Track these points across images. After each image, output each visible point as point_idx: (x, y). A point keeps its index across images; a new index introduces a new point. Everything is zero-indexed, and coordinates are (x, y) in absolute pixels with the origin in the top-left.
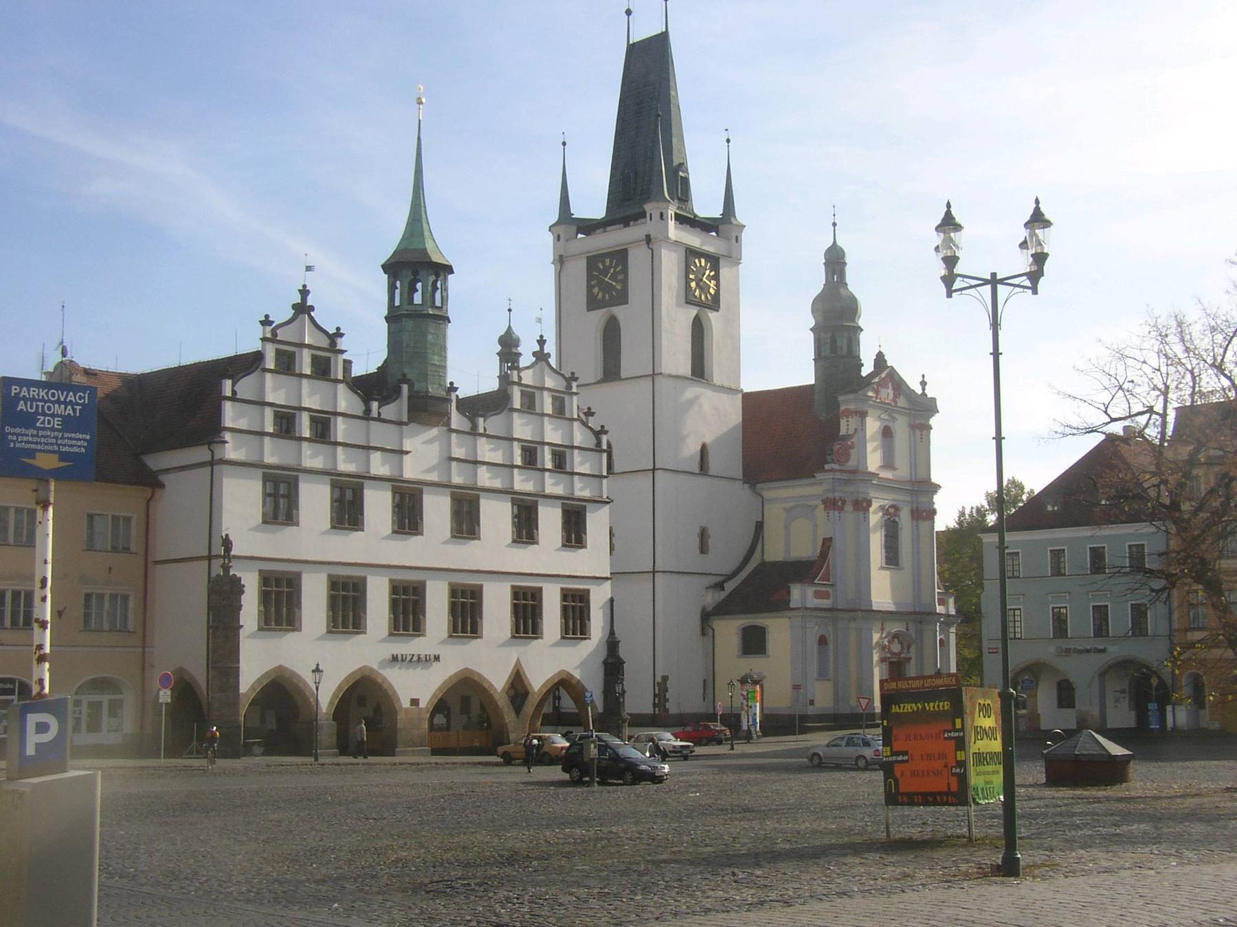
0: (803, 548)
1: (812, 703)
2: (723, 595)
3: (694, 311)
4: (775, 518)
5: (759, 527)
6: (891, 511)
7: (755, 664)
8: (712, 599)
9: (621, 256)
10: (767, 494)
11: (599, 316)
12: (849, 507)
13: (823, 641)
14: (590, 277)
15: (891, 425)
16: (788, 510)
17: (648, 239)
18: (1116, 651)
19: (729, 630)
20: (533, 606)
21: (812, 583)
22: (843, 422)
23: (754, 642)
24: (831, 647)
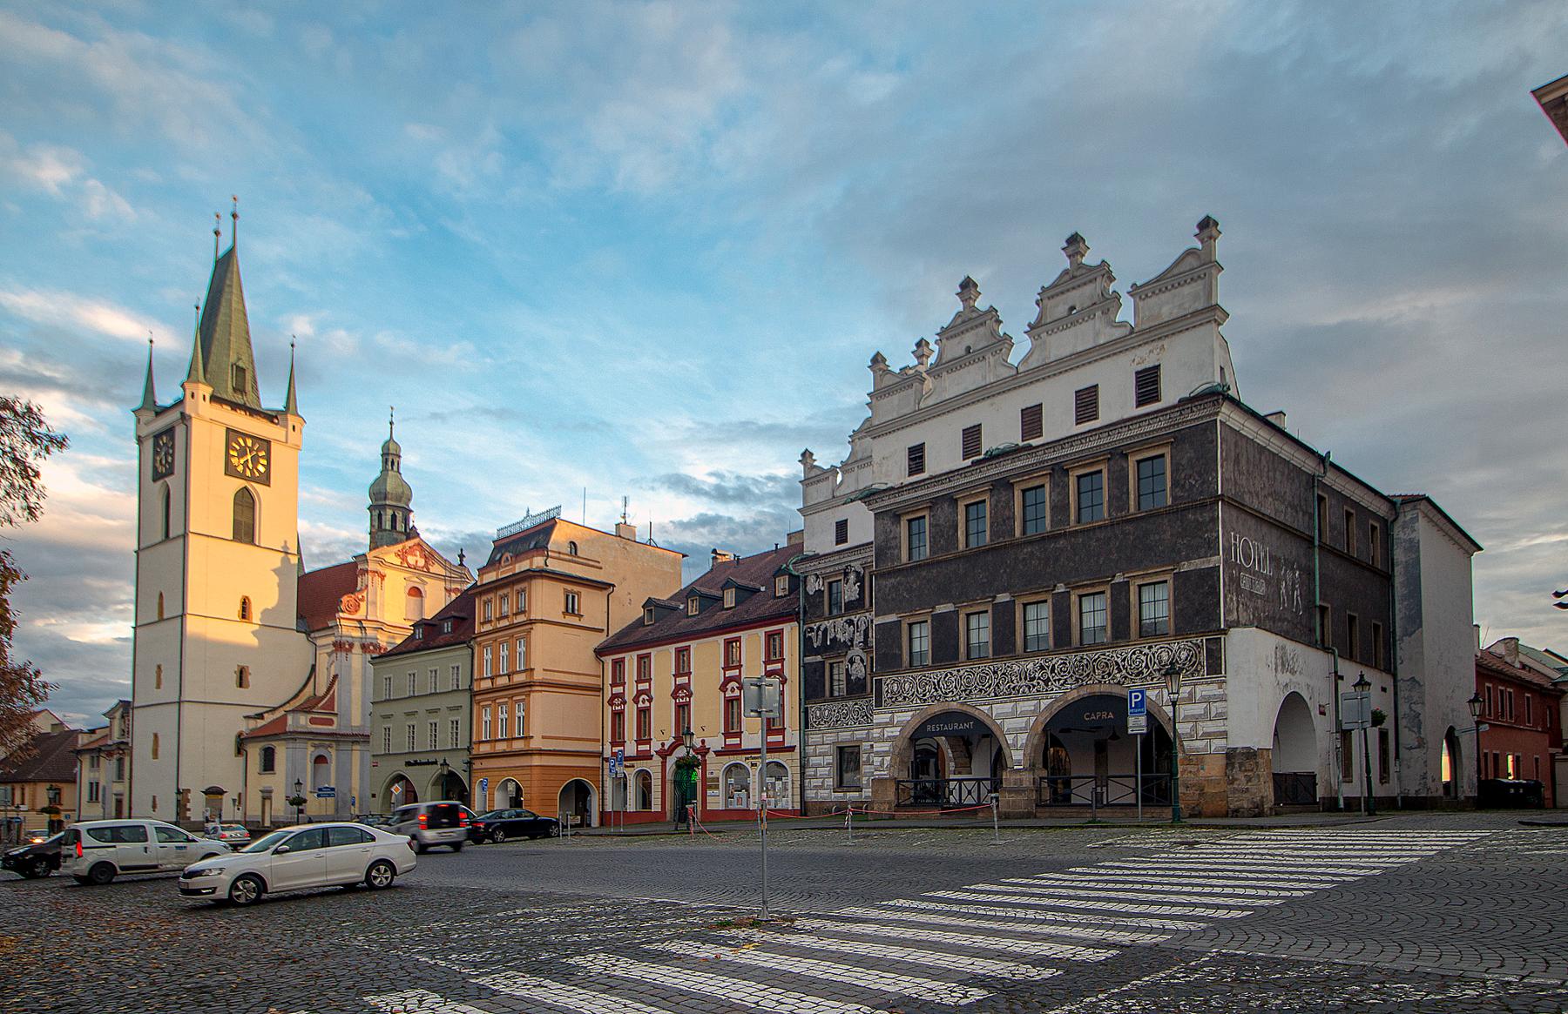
2: (260, 723)
7: (268, 781)
8: (245, 727)
14: (156, 453)
19: (255, 752)
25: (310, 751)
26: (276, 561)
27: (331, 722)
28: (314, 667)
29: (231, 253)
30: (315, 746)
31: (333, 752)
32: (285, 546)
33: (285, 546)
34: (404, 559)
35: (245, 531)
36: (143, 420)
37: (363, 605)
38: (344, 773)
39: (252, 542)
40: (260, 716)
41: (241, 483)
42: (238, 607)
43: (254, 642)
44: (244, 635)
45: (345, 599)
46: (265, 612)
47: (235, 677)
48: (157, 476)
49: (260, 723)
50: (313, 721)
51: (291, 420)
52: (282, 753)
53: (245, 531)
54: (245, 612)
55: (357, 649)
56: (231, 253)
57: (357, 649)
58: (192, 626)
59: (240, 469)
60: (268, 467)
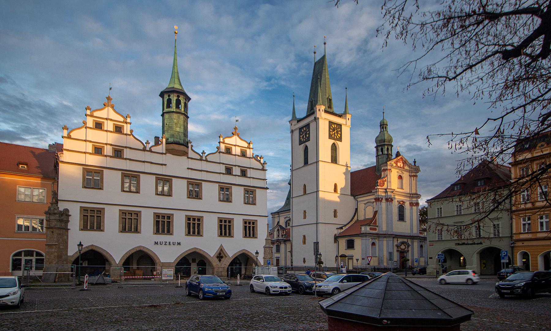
0: (370, 215)
2: (342, 231)
3: (332, 141)
4: (361, 206)
5: (357, 209)
6: (401, 203)
8: (337, 232)
9: (308, 126)
10: (359, 200)
16: (365, 204)
18: (487, 244)
19: (343, 243)
23: (350, 245)
26: (344, 169)
32: (347, 164)
33: (347, 164)
34: (397, 164)
35: (334, 160)
37: (386, 183)
38: (381, 250)
39: (336, 163)
40: (341, 228)
41: (333, 141)
42: (333, 188)
43: (338, 200)
44: (335, 198)
45: (379, 181)
46: (341, 189)
47: (333, 213)
48: (301, 143)
49: (342, 231)
53: (334, 160)
54: (335, 190)
55: (384, 201)
57: (384, 201)
58: (321, 195)
59: (333, 136)
60: (341, 134)
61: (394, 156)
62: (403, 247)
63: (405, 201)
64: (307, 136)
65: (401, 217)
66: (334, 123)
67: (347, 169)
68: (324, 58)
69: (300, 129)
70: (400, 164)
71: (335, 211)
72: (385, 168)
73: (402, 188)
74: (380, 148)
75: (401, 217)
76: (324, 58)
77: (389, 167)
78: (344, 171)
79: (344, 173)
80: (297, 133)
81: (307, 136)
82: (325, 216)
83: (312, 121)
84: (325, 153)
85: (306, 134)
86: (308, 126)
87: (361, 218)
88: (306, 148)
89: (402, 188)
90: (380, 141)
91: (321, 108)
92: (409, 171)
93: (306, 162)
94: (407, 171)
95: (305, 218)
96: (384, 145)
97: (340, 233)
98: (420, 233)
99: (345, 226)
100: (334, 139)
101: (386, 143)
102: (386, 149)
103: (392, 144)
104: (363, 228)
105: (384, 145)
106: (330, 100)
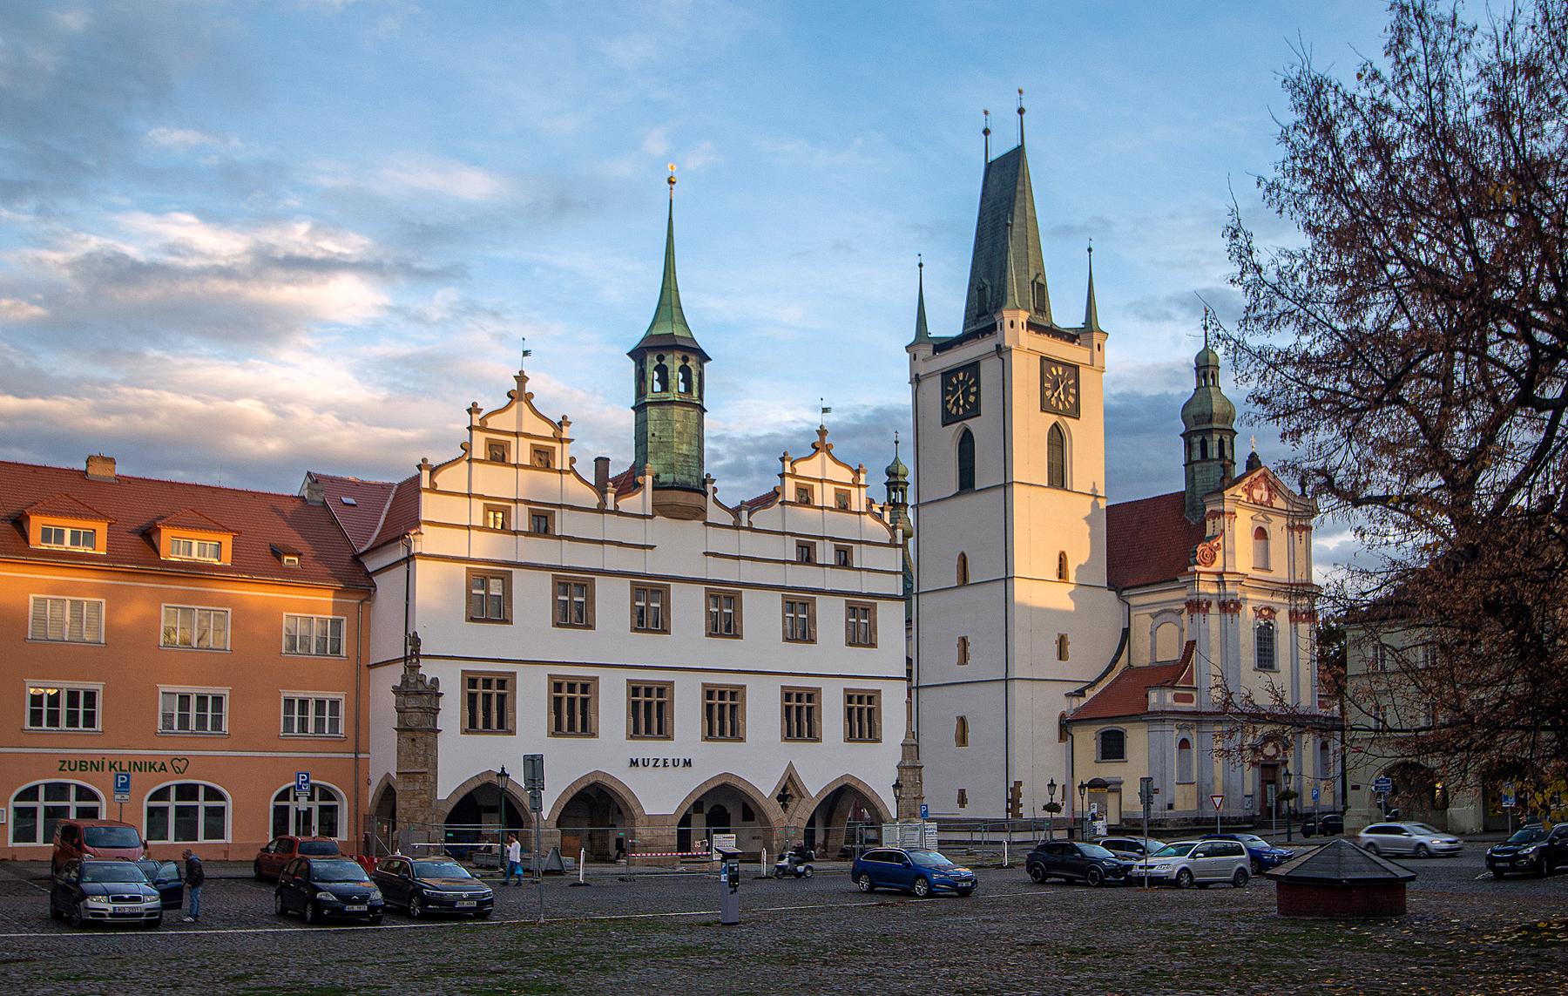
0: (1170, 652)
1: (1171, 807)
2: (1083, 701)
4: (1142, 623)
5: (1126, 633)
6: (1265, 613)
7: (1110, 771)
9: (973, 368)
10: (1134, 601)
11: (955, 429)
12: (1214, 609)
13: (1184, 744)
14: (945, 392)
15: (1264, 526)
17: (999, 349)
19: (1087, 740)
20: (809, 709)
21: (1173, 687)
22: (1209, 524)
23: (1112, 747)
24: (1195, 750)
25: (1173, 735)
27: (1189, 699)
28: (1126, 633)
29: (1017, 155)
30: (1180, 729)
31: (1194, 732)
32: (1094, 489)
33: (1094, 489)
34: (1250, 495)
36: (921, 355)
39: (1062, 486)
40: (1081, 693)
41: (1053, 418)
43: (1070, 605)
44: (1059, 597)
47: (1056, 647)
48: (948, 419)
50: (1177, 698)
51: (1096, 337)
52: (1137, 739)
54: (1062, 574)
56: (1017, 155)
60: (1077, 396)
61: (1239, 469)
62: (1269, 750)
63: (1276, 607)
64: (972, 399)
65: (1266, 659)
66: (1057, 363)
67: (1095, 506)
68: (1019, 152)
69: (947, 375)
70: (1260, 493)
71: (1062, 641)
72: (1218, 508)
73: (1267, 569)
74: (1197, 440)
75: (1266, 659)
76: (1019, 152)
77: (1228, 507)
78: (1088, 511)
79: (1088, 519)
80: (934, 388)
81: (972, 399)
82: (1033, 655)
83: (987, 356)
84: (1029, 460)
85: (966, 394)
86: (973, 368)
87: (1142, 659)
88: (967, 441)
89: (1267, 569)
90: (1198, 419)
91: (1015, 318)
92: (1287, 514)
93: (967, 482)
94: (1279, 512)
95: (964, 659)
96: (1210, 431)
97: (1077, 710)
98: (1321, 705)
99: (1092, 685)
100: (1056, 412)
101: (1215, 425)
102: (1216, 443)
103: (1235, 426)
104: (1154, 697)
105: (1210, 431)
106: (1042, 288)
